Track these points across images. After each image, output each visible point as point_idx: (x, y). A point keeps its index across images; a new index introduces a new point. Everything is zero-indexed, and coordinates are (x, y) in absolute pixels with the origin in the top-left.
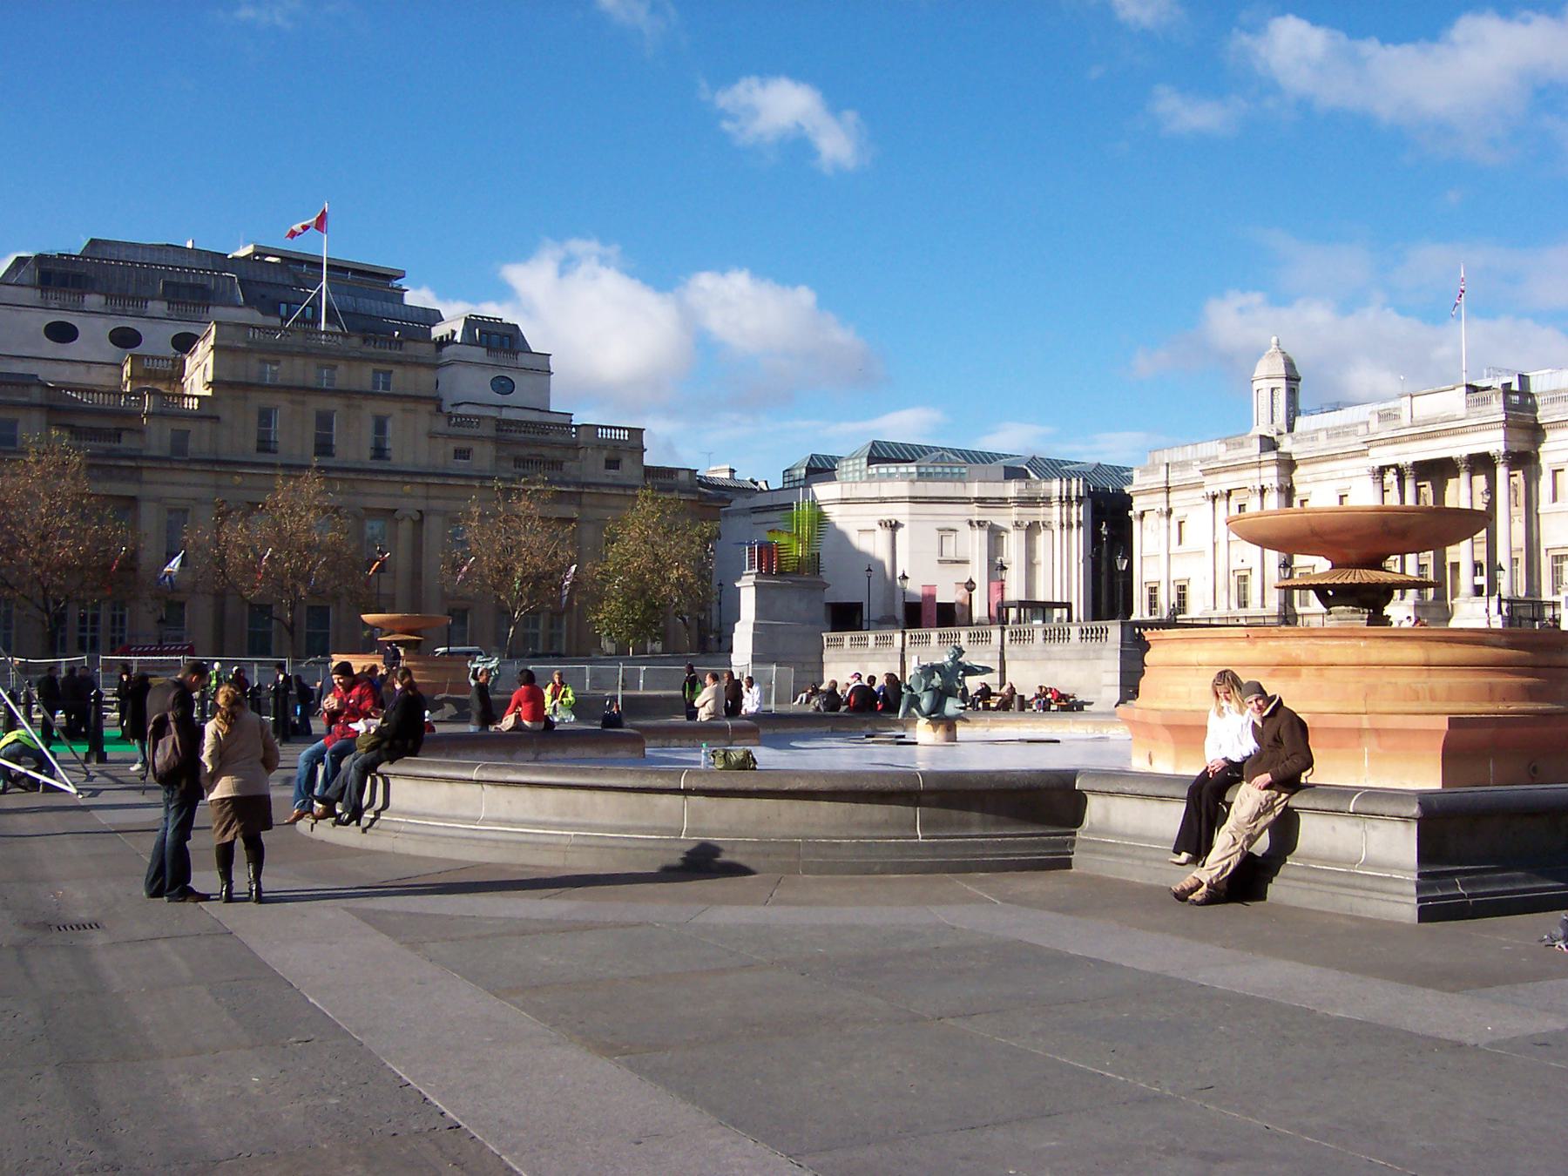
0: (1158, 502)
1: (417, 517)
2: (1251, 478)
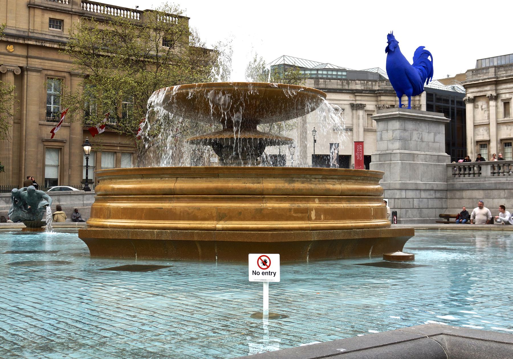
0: (489, 91)
1: (19, 72)
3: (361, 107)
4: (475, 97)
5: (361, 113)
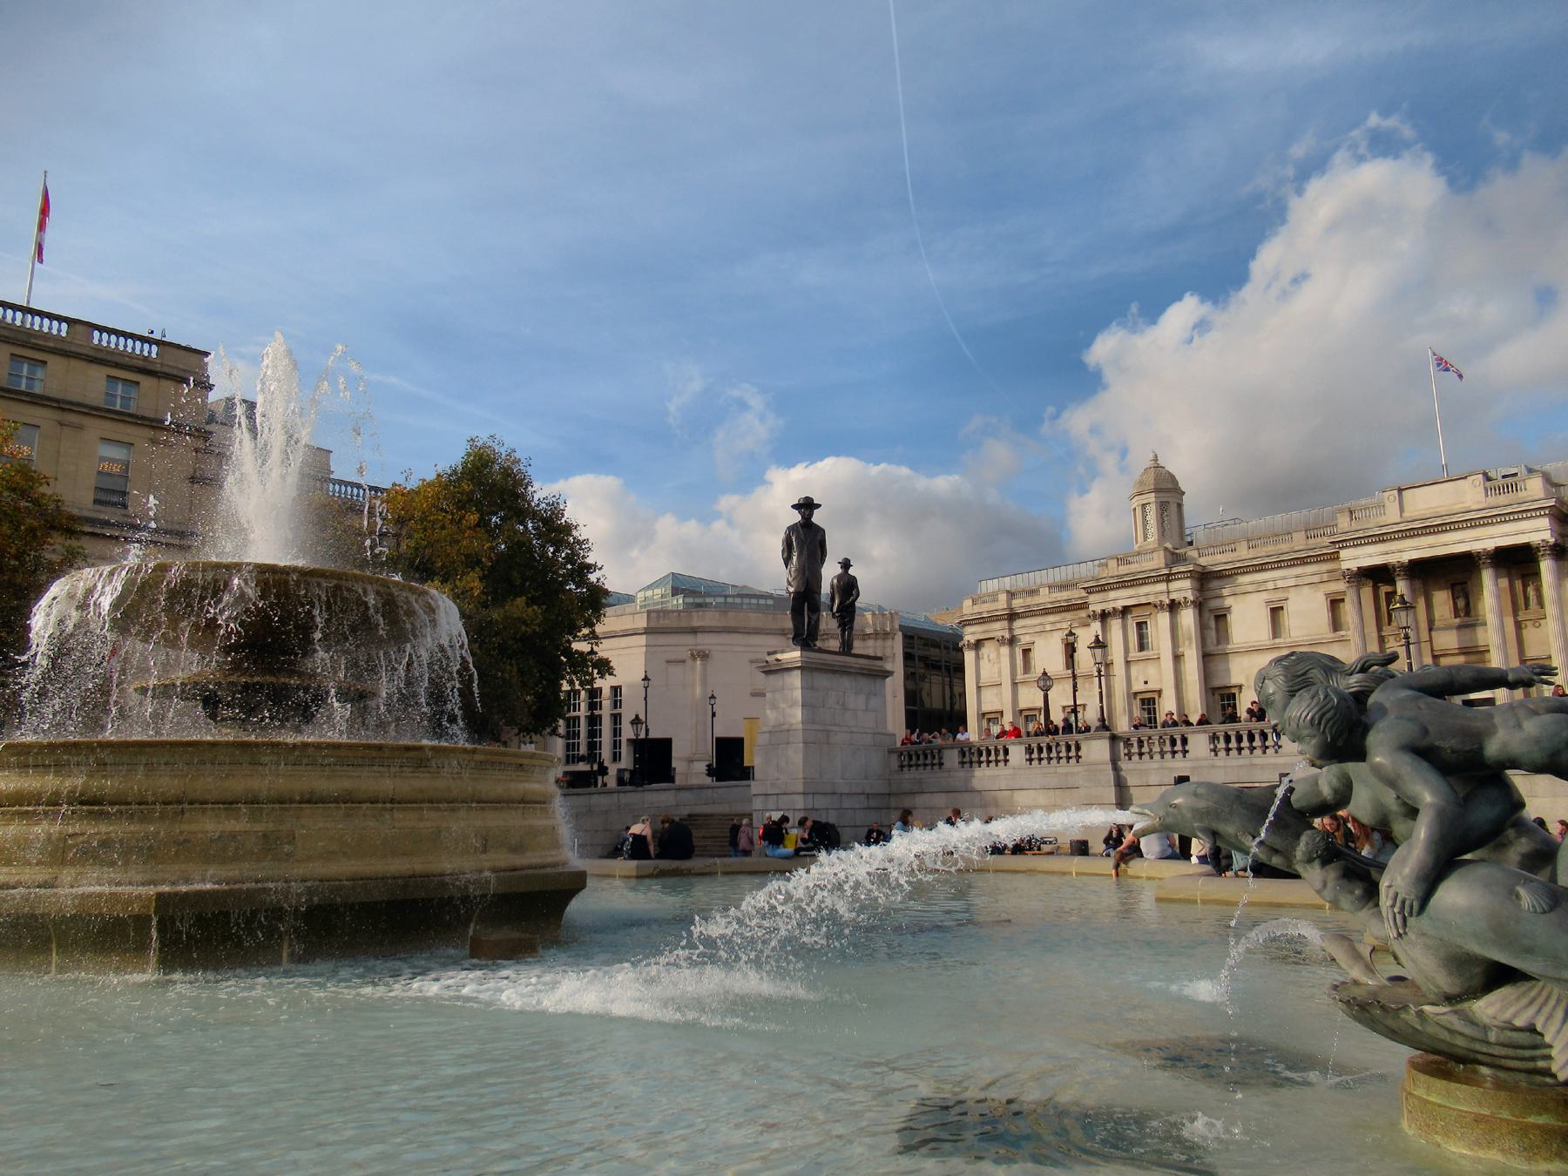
0: (999, 629)
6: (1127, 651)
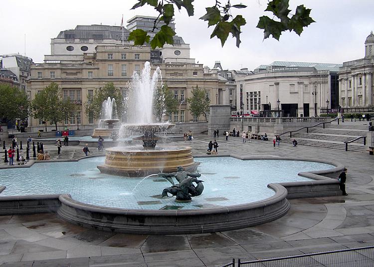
0: (345, 77)
2: (362, 71)
3: (302, 83)
4: (341, 79)
5: (302, 86)
6: (357, 85)
